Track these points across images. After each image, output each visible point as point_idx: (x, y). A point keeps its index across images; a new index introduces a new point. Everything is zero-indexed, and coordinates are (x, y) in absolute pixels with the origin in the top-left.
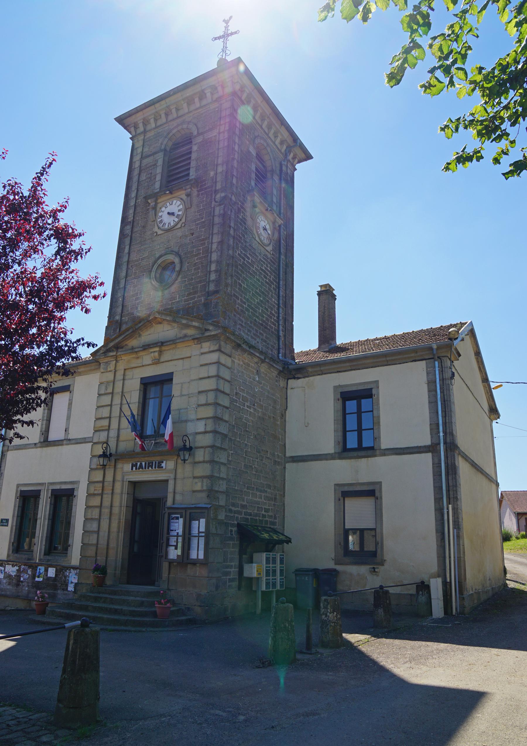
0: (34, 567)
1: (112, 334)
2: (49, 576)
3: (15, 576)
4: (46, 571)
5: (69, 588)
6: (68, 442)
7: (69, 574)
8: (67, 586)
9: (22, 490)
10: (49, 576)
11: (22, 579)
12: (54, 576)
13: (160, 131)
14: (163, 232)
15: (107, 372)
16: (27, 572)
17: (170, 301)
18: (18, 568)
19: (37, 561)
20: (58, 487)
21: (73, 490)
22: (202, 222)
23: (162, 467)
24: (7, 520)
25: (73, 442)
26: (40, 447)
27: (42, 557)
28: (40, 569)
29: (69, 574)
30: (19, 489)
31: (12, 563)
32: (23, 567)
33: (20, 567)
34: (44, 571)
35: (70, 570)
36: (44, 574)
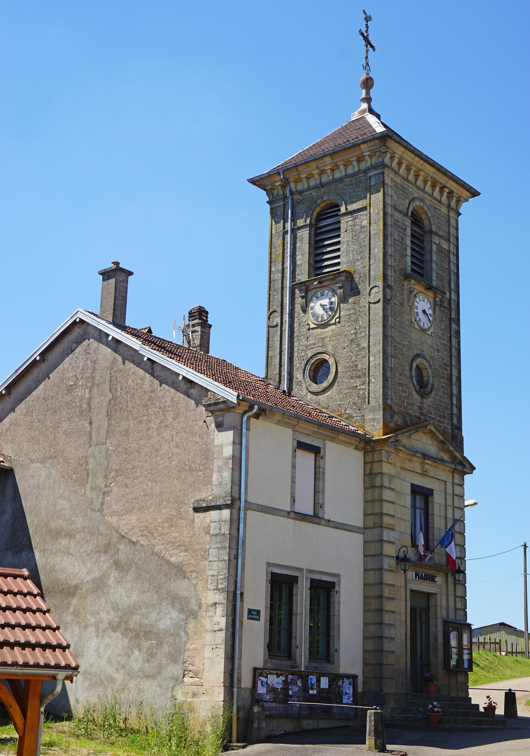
0: (304, 677)
1: (389, 420)
2: (322, 687)
3: (281, 689)
4: (318, 681)
5: (344, 700)
6: (327, 523)
7: (342, 684)
8: (341, 698)
9: (274, 571)
10: (322, 687)
11: (291, 693)
12: (327, 687)
13: (406, 186)
14: (418, 328)
15: (387, 463)
16: (297, 683)
17: (428, 413)
18: (284, 678)
19: (303, 669)
20: (317, 577)
21: (332, 585)
22: (443, 343)
23: (436, 582)
24: (258, 612)
25: (332, 524)
26: (294, 519)
27: (307, 664)
28: (311, 679)
29: (342, 684)
30: (270, 570)
31: (276, 672)
32: (290, 677)
33: (286, 677)
34: (315, 681)
35: (343, 679)
36: (316, 685)
